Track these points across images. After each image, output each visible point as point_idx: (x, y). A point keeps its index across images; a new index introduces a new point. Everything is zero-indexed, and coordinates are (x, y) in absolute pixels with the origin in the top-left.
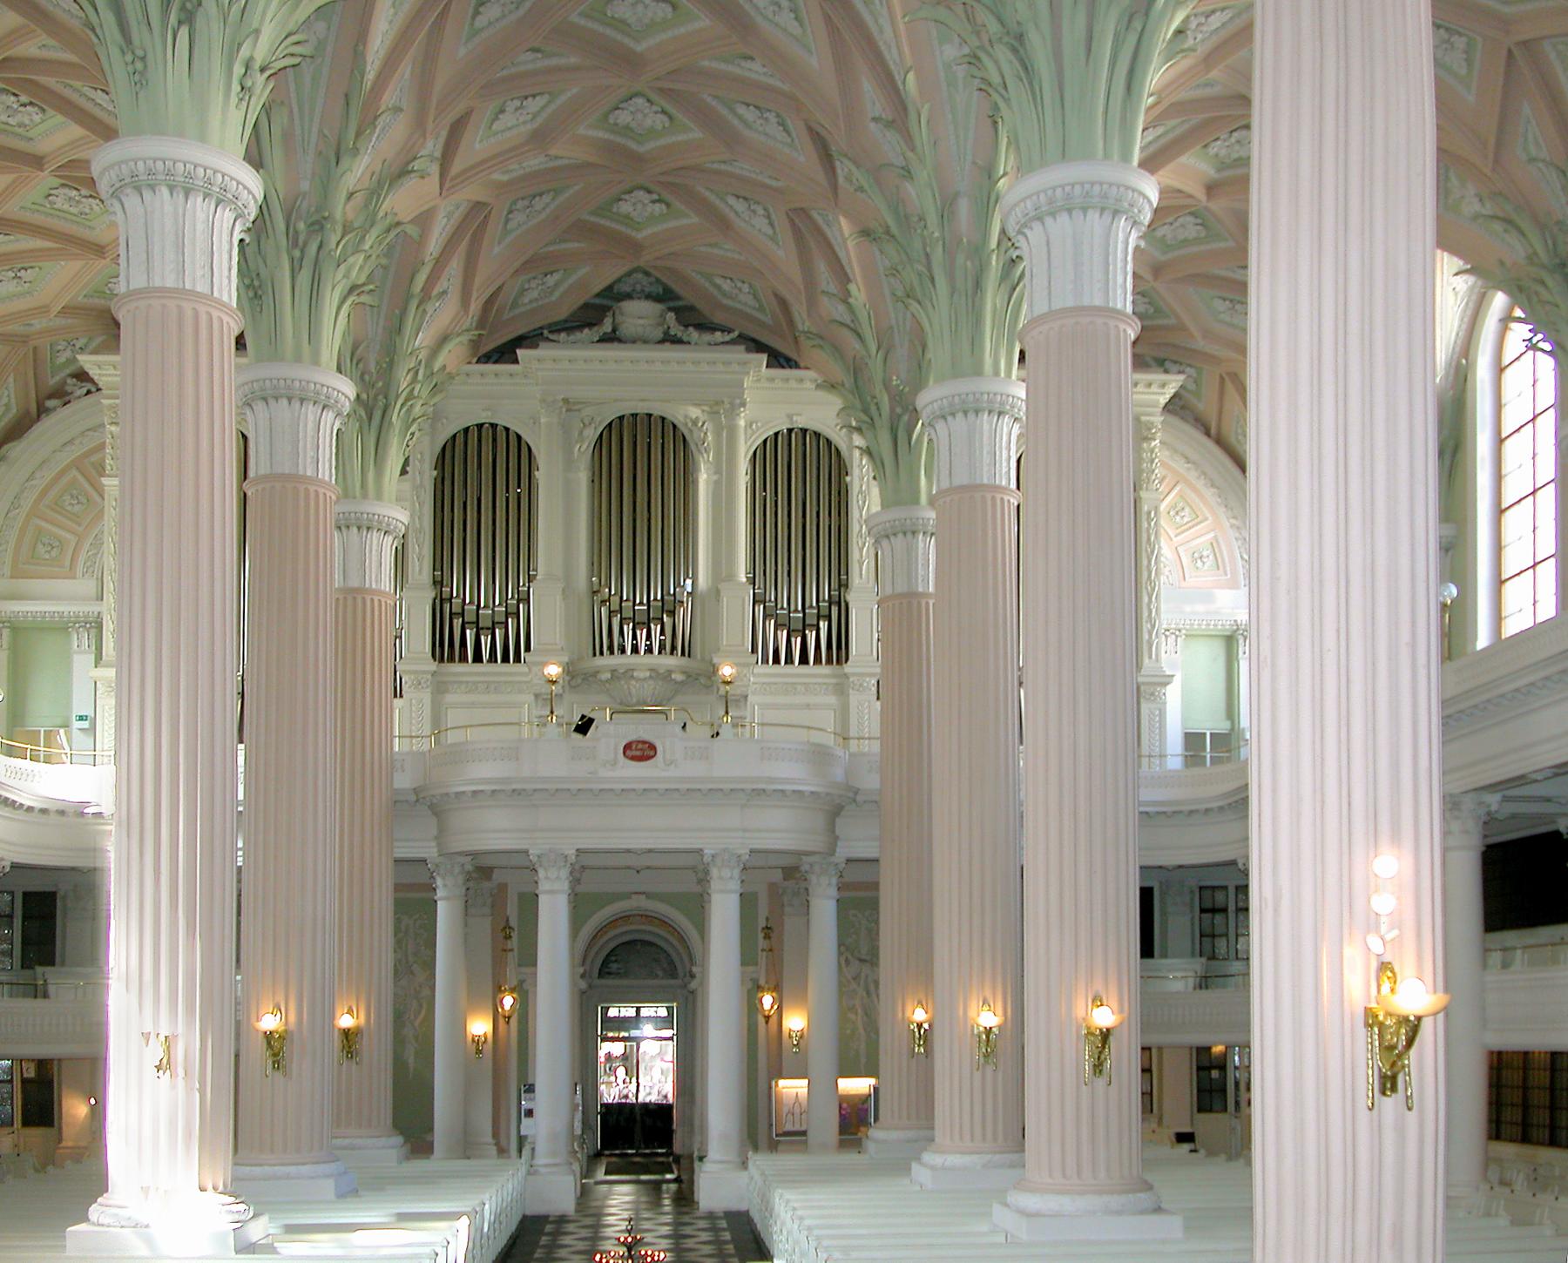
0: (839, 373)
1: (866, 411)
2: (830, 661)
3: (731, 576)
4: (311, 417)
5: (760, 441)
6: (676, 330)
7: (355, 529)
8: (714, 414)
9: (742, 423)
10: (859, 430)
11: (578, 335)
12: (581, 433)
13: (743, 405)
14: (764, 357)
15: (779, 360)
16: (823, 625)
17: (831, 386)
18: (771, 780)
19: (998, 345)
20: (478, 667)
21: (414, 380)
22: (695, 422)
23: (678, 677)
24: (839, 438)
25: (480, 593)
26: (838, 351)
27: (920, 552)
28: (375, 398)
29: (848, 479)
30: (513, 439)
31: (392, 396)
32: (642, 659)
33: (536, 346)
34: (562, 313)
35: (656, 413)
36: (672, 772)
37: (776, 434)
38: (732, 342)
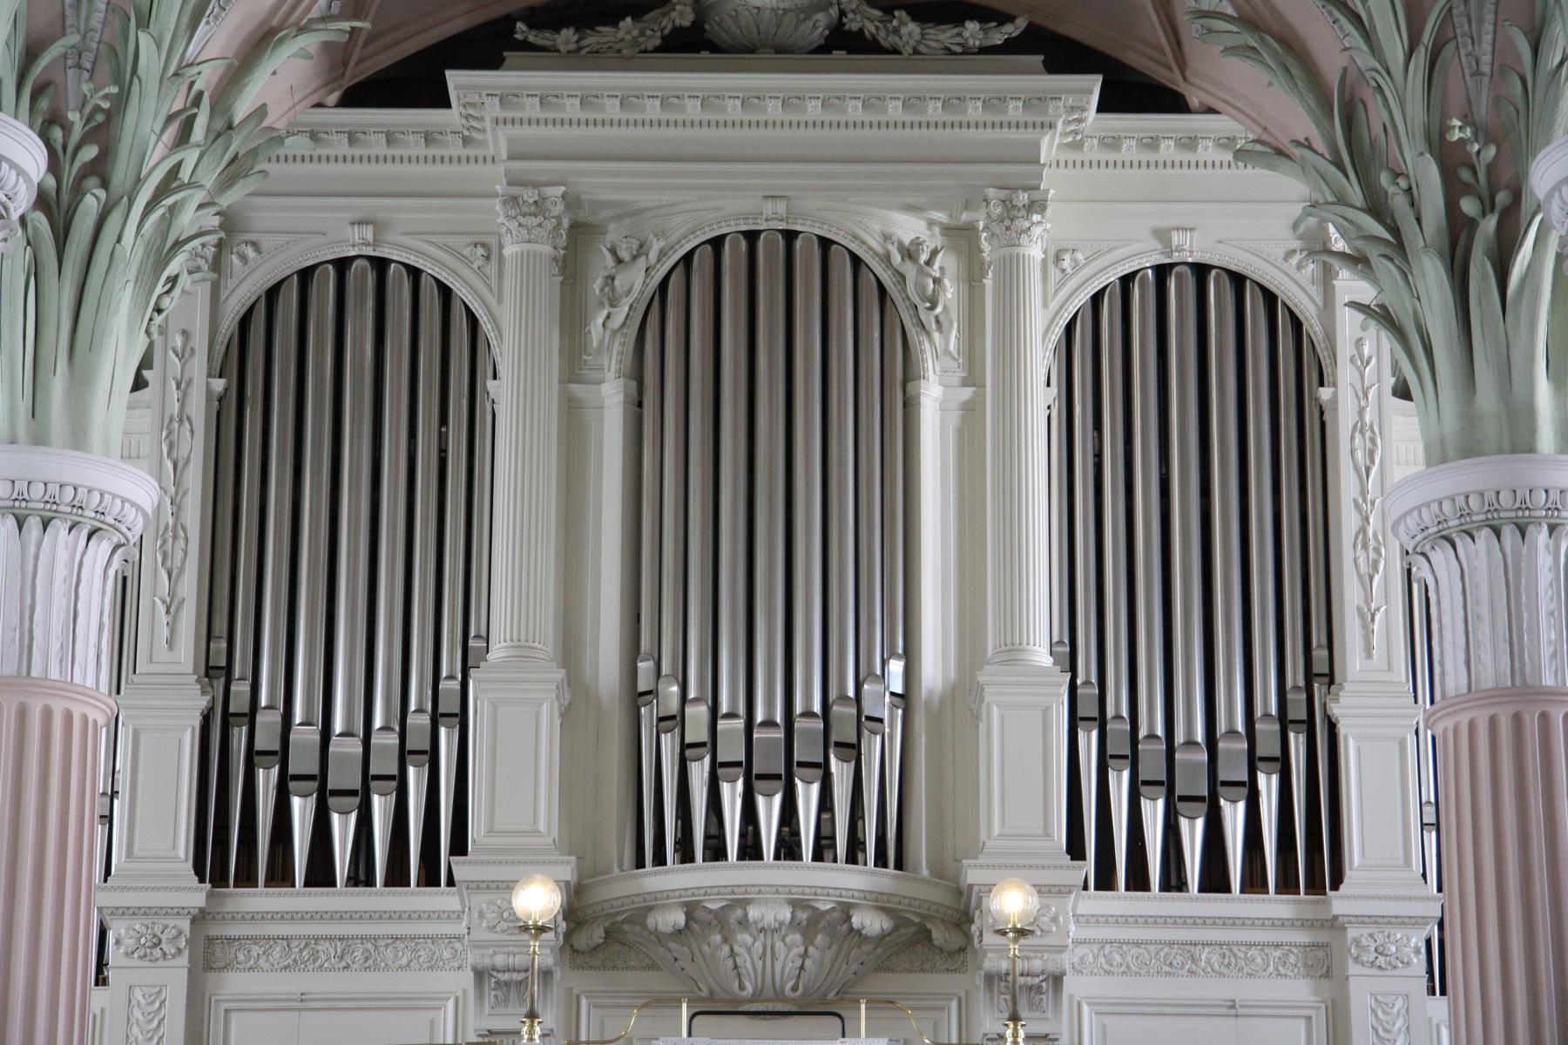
0: (1295, 117)
1: (1377, 208)
8: (961, 237)
9: (1034, 251)
10: (1358, 261)
11: (604, 35)
14: (1094, 84)
17: (1274, 153)
21: (183, 138)
22: (909, 253)
23: (870, 922)
24: (1296, 286)
25: (336, 705)
26: (1294, 55)
31: (120, 175)
32: (770, 872)
33: (494, 63)
37: (1127, 281)
38: (1010, 47)
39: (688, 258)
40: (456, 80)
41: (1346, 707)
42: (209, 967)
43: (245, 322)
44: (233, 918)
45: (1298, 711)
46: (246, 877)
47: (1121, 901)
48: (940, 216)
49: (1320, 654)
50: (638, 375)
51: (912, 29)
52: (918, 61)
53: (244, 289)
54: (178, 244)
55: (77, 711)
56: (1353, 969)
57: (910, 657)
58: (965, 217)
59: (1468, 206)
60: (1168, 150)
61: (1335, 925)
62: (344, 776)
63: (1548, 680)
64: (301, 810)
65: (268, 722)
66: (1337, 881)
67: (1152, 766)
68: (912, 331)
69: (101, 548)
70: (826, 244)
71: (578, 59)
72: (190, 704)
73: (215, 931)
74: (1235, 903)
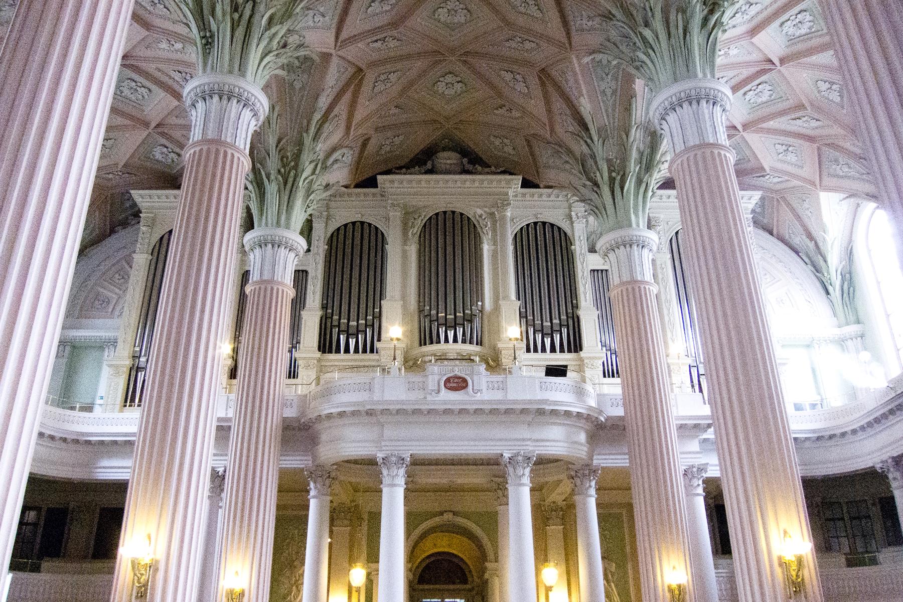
3: (506, 297)
4: (234, 110)
6: (470, 167)
7: (270, 246)
11: (413, 170)
12: (413, 223)
15: (526, 184)
16: (564, 331)
18: (545, 401)
19: (704, 70)
20: (347, 356)
22: (481, 216)
24: (565, 226)
28: (289, 172)
29: (573, 247)
30: (373, 230)
31: (301, 167)
32: (451, 346)
35: (458, 210)
36: (478, 396)
37: (528, 225)
39: (430, 218)
40: (379, 177)
46: (330, 352)
47: (532, 355)
48: (486, 209)
49: (574, 302)
51: (479, 168)
55: (285, 290)
56: (586, 369)
58: (493, 210)
59: (614, 174)
60: (536, 198)
61: (581, 360)
63: (639, 279)
64: (342, 338)
65: (336, 317)
66: (581, 350)
67: (538, 327)
68: (481, 234)
69: (292, 255)
70: (462, 214)
71: (405, 174)
72: (319, 313)
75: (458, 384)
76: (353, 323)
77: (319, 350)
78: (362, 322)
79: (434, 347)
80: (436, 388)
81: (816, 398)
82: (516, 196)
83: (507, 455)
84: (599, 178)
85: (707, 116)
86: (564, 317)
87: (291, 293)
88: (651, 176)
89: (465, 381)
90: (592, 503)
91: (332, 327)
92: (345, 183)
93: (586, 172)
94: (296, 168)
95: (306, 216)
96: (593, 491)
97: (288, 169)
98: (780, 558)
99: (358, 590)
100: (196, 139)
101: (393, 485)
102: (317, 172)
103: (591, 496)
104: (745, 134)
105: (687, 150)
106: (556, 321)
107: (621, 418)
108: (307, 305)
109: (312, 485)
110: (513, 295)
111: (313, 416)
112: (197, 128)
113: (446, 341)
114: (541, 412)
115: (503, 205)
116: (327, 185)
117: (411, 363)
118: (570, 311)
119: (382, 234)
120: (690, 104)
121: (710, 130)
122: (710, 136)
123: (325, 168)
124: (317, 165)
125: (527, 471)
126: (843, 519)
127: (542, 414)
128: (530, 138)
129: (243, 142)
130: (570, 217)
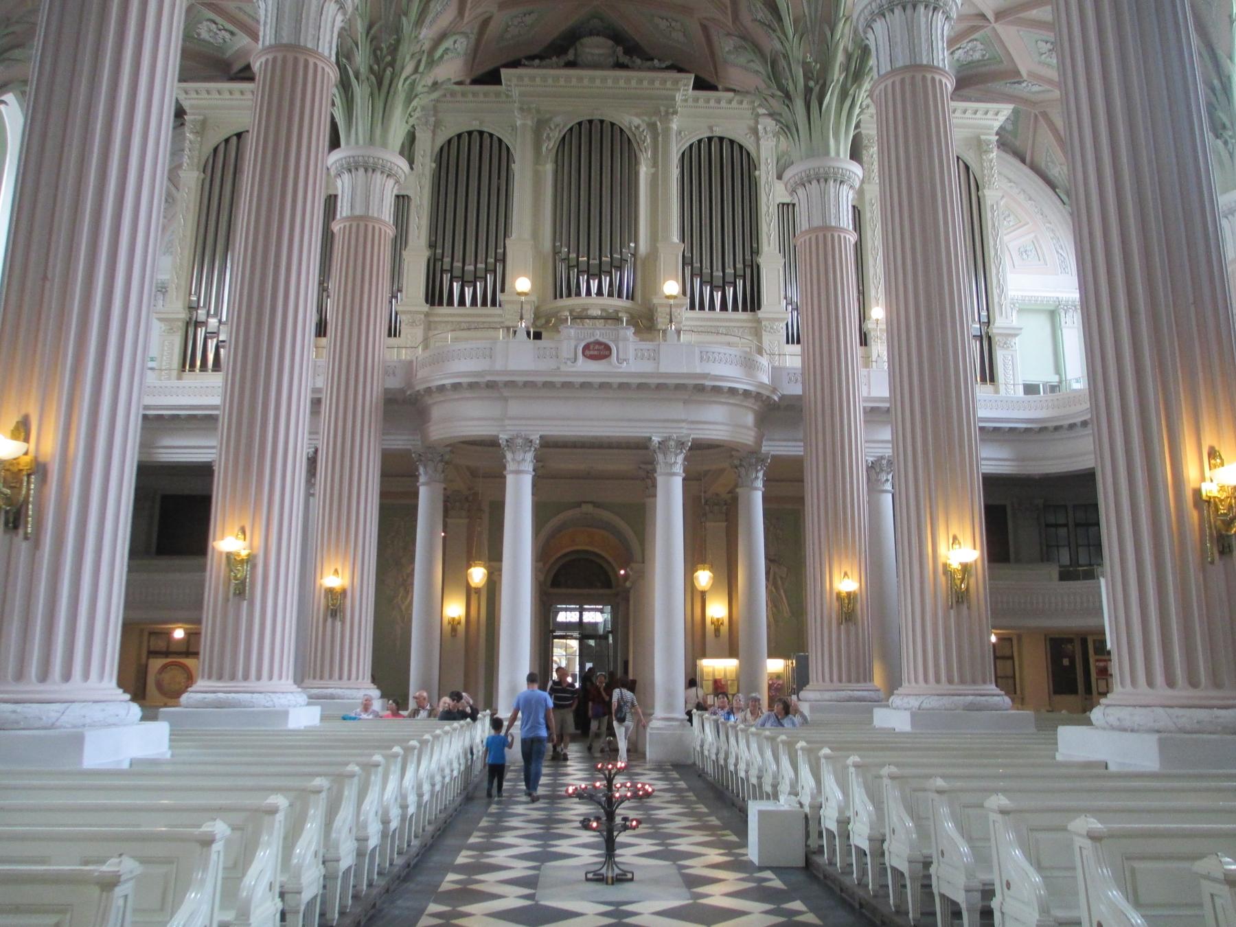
2: (744, 309)
5: (688, 145)
6: (625, 59)
7: (361, 171)
8: (652, 126)
13: (675, 113)
15: (701, 85)
16: (740, 283)
18: (705, 376)
20: (462, 310)
22: (637, 127)
24: (749, 144)
27: (832, 195)
28: (384, 70)
29: (757, 173)
31: (398, 63)
34: (536, 50)
35: (607, 119)
36: (624, 367)
37: (700, 141)
39: (571, 129)
41: (763, 260)
42: (429, 329)
43: (441, 149)
44: (437, 315)
45: (748, 263)
46: (441, 304)
47: (697, 313)
48: (646, 118)
49: (755, 245)
50: (556, 162)
51: (638, 61)
52: (640, 69)
53: (441, 140)
54: (416, 96)
57: (636, 242)
58: (654, 119)
59: (811, 84)
60: (712, 103)
61: (759, 321)
62: (469, 277)
64: (456, 286)
65: (447, 260)
66: (759, 308)
69: (391, 182)
70: (612, 124)
71: (538, 67)
73: (431, 319)
74: (730, 314)
75: (598, 351)
76: (470, 268)
77: (427, 301)
78: (481, 266)
79: (573, 301)
80: (572, 355)
81: (1054, 379)
82: (686, 100)
83: (656, 439)
84: (791, 88)
85: (923, 26)
86: (739, 266)
87: (390, 232)
88: (860, 87)
89: (608, 348)
90: (758, 497)
91: (442, 271)
92: (458, 79)
93: (775, 75)
94: (392, 64)
95: (408, 127)
96: (759, 484)
97: (382, 66)
98: (945, 566)
99: (478, 591)
100: (267, 43)
101: (518, 472)
102: (421, 69)
103: (756, 489)
104: (997, 26)
105: (894, 71)
106: (730, 271)
107: (799, 398)
108: (410, 242)
109: (421, 470)
110: (675, 239)
111: (421, 387)
112: (268, 27)
113: (589, 293)
114: (700, 389)
115: (667, 113)
116: (435, 84)
117: (543, 321)
118: (748, 257)
119: (508, 148)
120: (904, 9)
121: (924, 46)
122: (924, 54)
123: (431, 63)
124: (420, 61)
125: (680, 459)
126: (1066, 525)
127: (700, 391)
128: (706, 22)
129: (327, 46)
130: (755, 132)
